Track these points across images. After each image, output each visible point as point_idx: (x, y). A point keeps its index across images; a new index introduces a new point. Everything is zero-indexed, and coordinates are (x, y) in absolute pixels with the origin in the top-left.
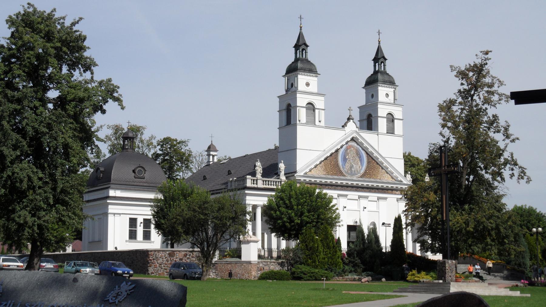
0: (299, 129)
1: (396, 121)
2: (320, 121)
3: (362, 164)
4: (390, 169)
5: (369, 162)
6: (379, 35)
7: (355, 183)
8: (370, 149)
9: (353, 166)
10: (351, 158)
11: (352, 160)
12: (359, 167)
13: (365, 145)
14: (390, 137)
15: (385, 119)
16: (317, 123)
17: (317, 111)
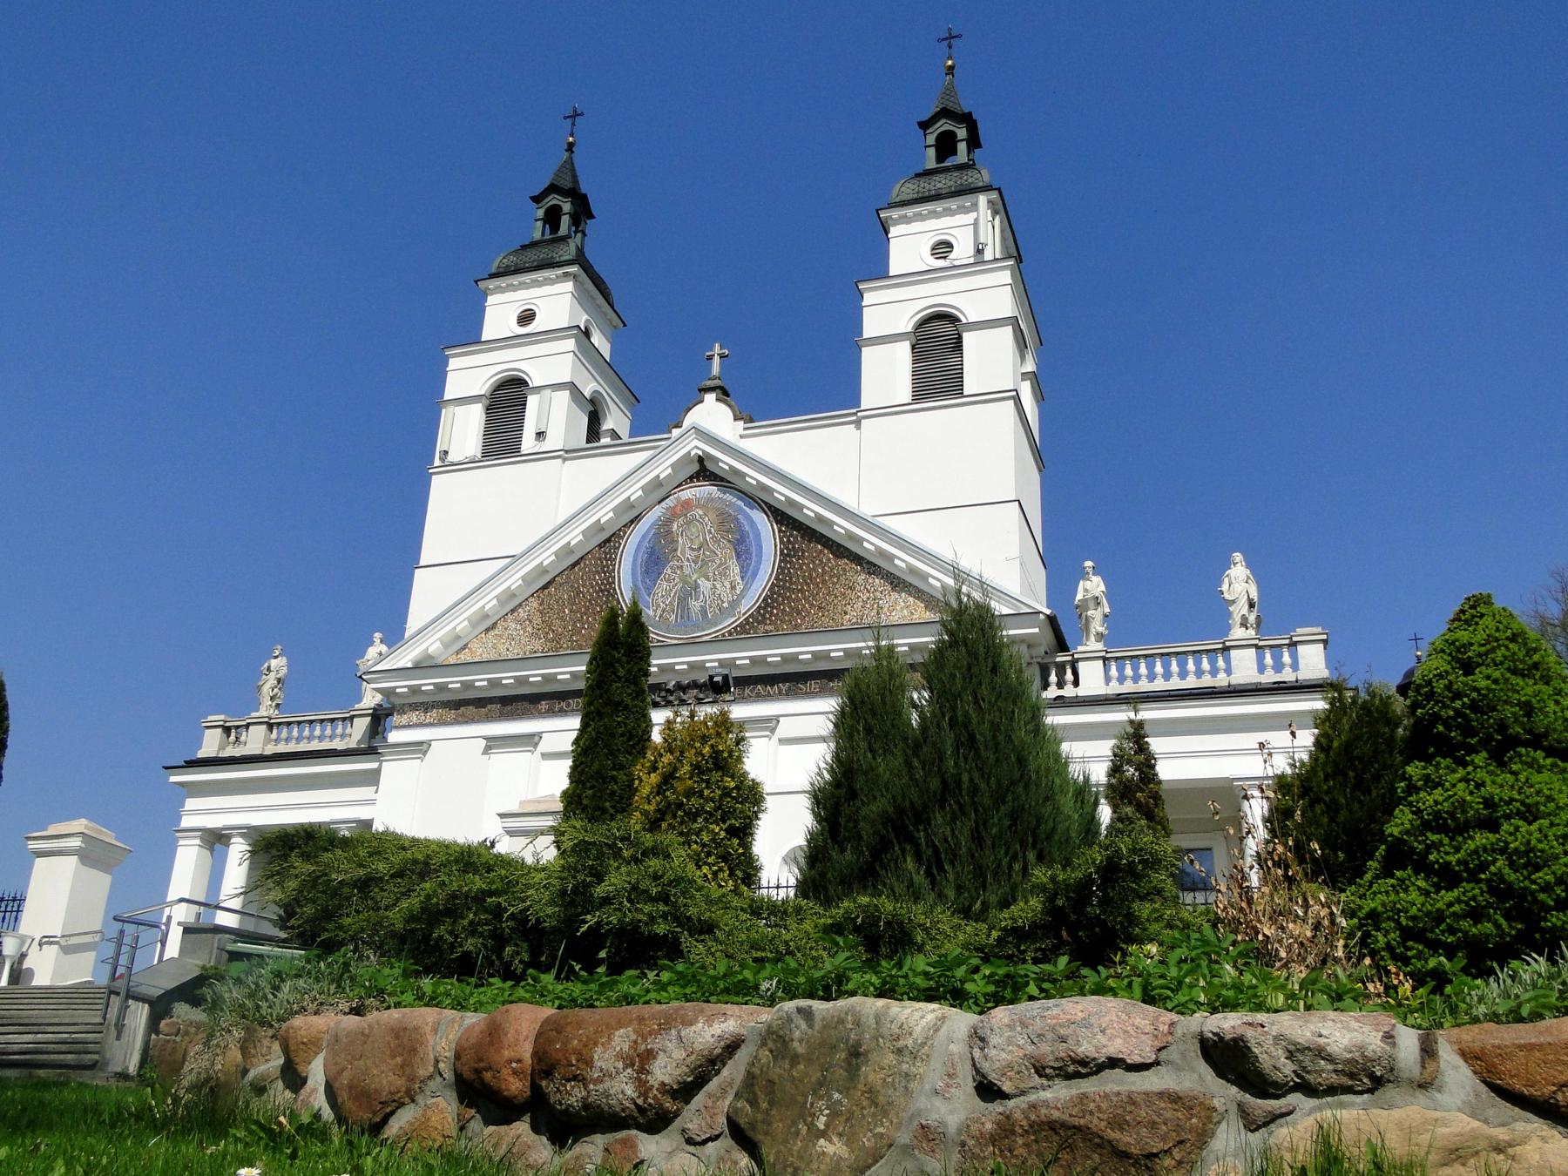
0: (441, 487)
1: (968, 338)
2: (540, 435)
3: (748, 573)
4: (903, 560)
5: (787, 556)
6: (950, 47)
7: (712, 660)
8: (782, 492)
9: (696, 587)
10: (688, 553)
11: (695, 562)
12: (733, 588)
13: (754, 476)
14: (941, 419)
15: (904, 350)
16: (528, 443)
17: (532, 401)
